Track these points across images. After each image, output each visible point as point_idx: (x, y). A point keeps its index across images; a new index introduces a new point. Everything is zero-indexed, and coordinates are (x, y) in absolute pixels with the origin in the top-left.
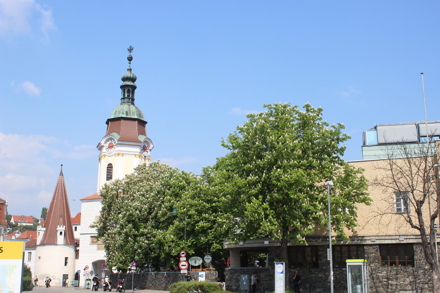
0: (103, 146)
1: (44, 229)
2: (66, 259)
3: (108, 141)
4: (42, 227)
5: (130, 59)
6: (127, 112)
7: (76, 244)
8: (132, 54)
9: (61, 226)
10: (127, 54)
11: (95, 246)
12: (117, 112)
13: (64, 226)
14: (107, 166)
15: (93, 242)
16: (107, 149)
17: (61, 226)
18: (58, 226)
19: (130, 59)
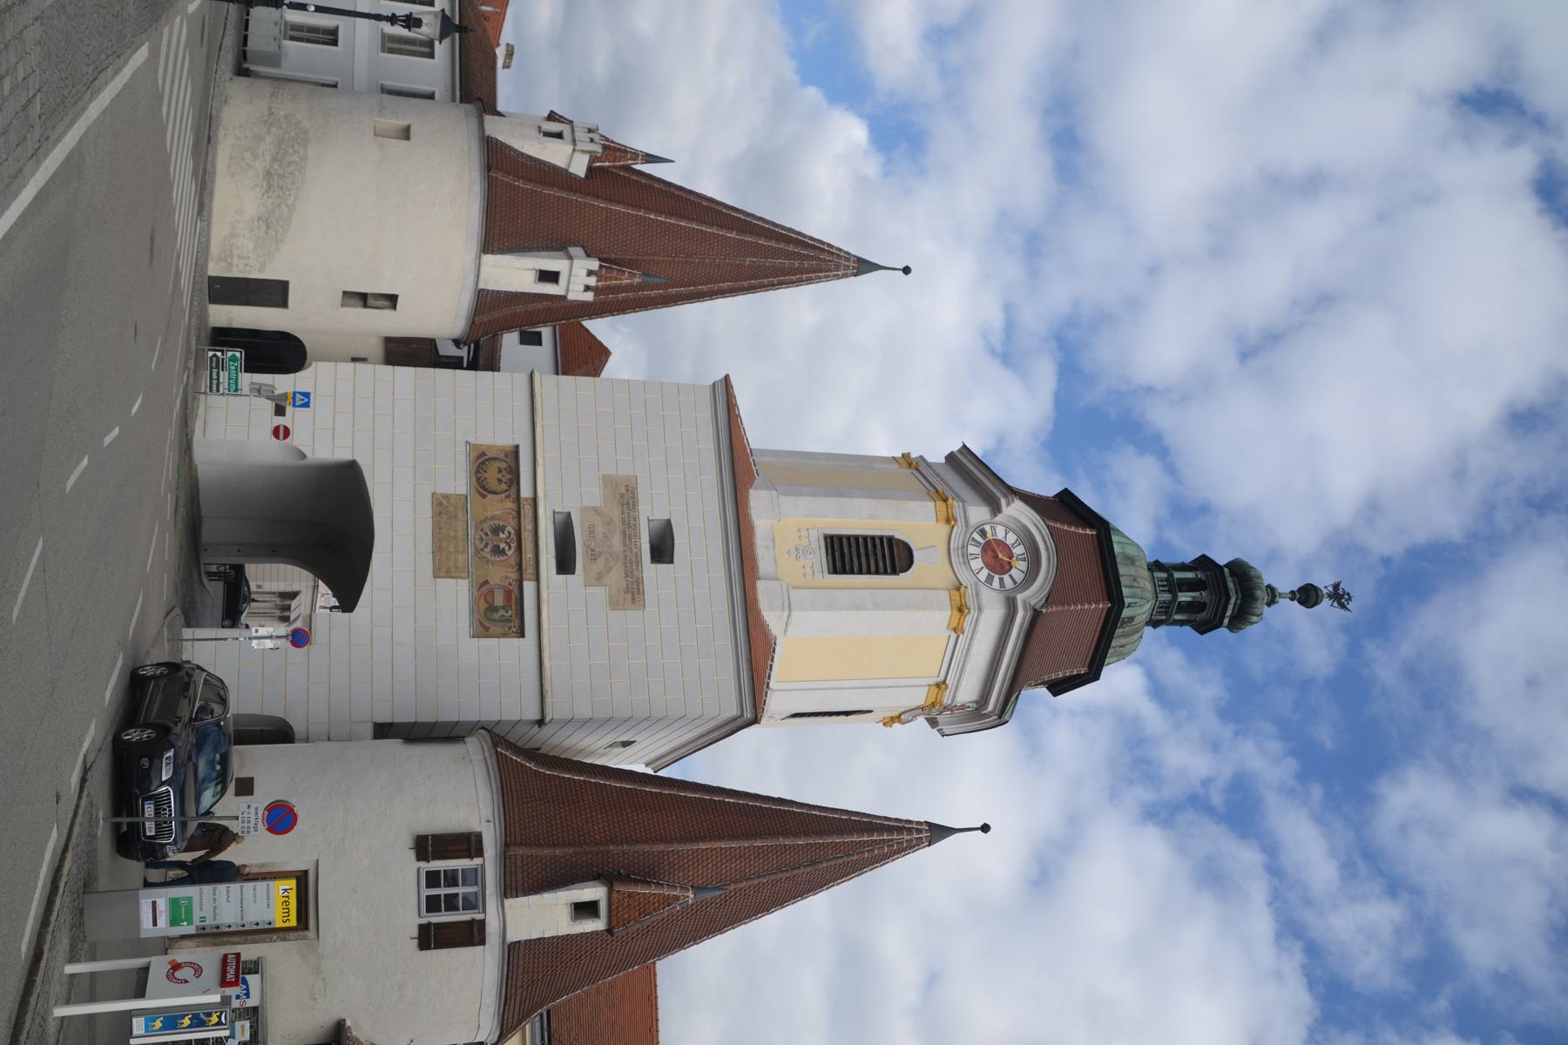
0: (996, 509)
1: (579, 168)
2: (392, 300)
3: (1020, 541)
4: (593, 159)
5: (1307, 596)
6: (1131, 619)
7: (478, 352)
8: (1326, 602)
9: (592, 281)
10: (1323, 581)
11: (459, 483)
12: (1132, 570)
13: (589, 296)
14: (897, 536)
15: (481, 461)
16: (983, 533)
17: (592, 281)
18: (594, 264)
19: (1307, 596)
